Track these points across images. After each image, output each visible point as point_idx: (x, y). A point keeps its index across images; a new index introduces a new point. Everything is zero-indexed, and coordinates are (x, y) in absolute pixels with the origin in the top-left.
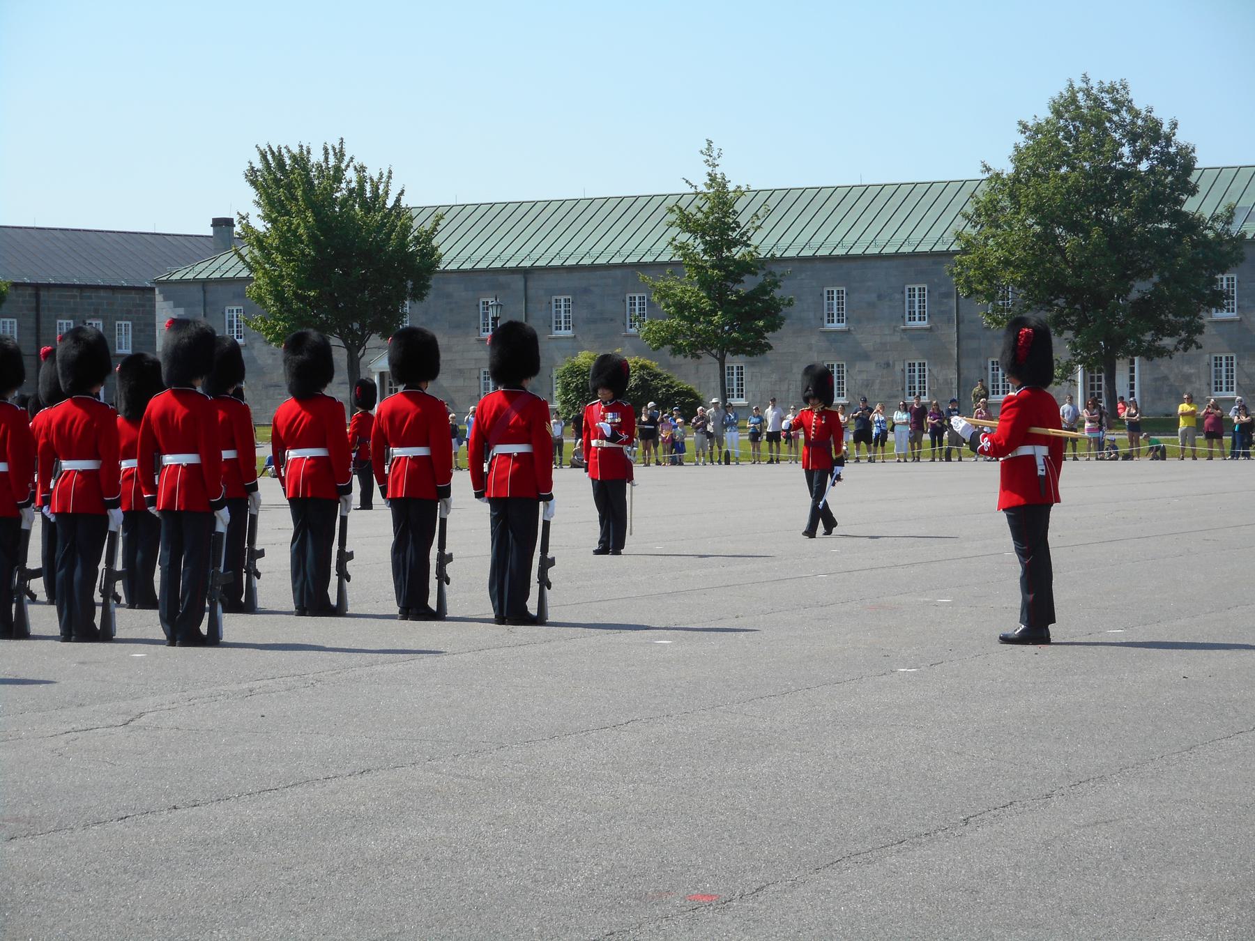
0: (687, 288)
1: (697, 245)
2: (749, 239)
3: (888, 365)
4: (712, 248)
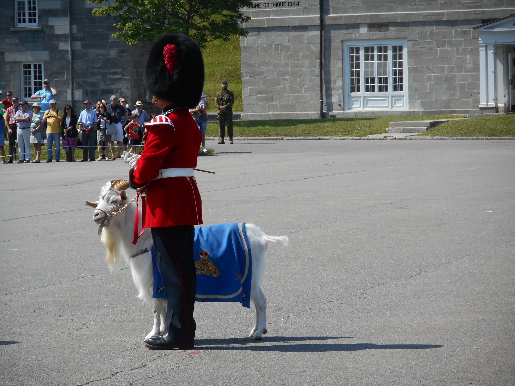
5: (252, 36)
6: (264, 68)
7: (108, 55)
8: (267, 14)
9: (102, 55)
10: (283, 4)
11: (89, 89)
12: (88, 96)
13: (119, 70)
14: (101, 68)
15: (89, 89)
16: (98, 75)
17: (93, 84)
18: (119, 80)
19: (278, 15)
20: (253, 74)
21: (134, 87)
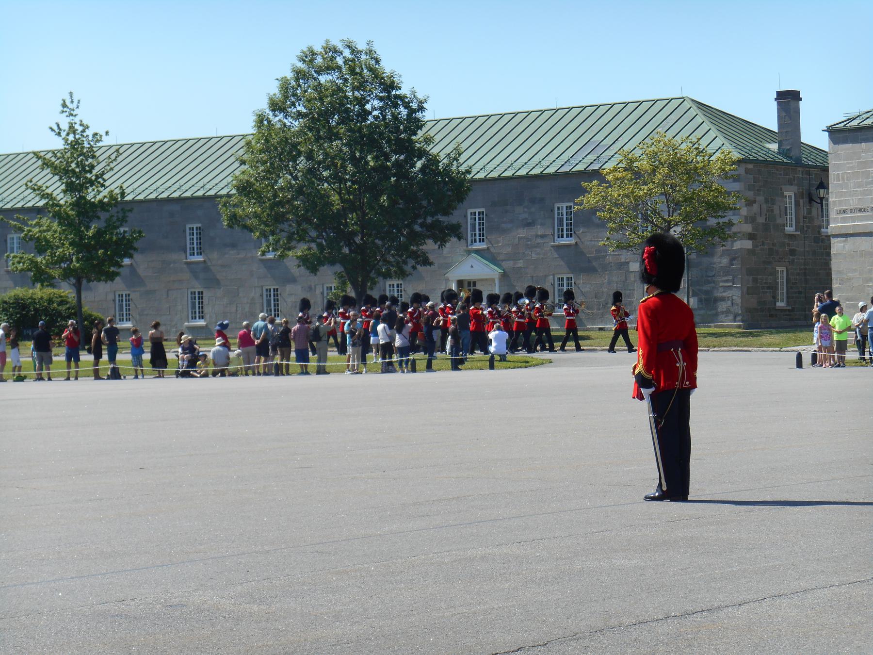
0: (49, 228)
1: (56, 187)
2: (105, 180)
3: (310, 288)
4: (70, 188)
5: (840, 242)
6: (850, 275)
7: (720, 263)
8: (853, 219)
10: (866, 210)
13: (730, 278)
15: (703, 296)
17: (707, 292)
19: (862, 221)
20: (842, 281)
21: (748, 294)
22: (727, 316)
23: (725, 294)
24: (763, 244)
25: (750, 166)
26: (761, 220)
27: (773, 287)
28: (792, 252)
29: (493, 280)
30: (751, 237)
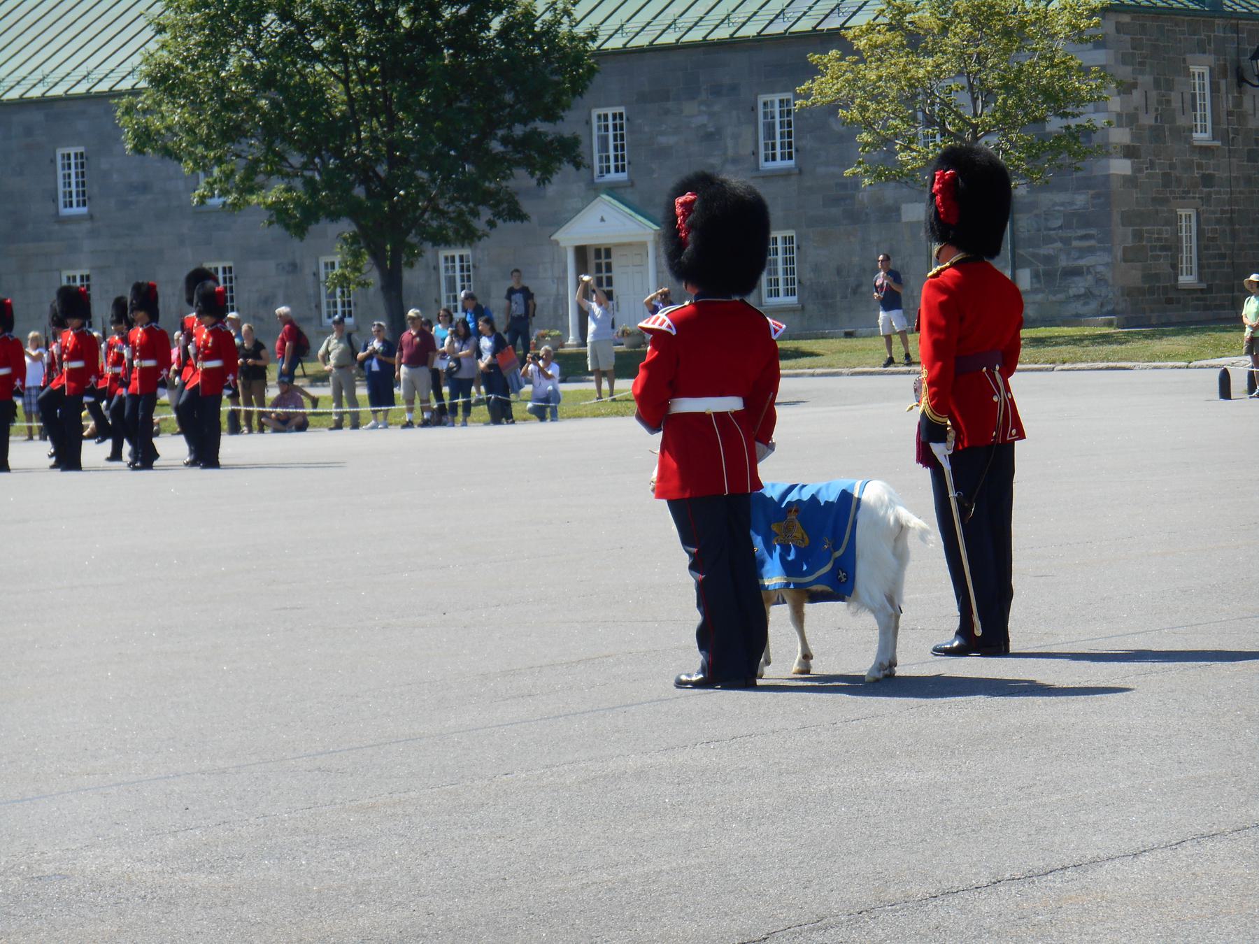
7: (1072, 203)
9: (1062, 204)
11: (1041, 268)
12: (1039, 281)
13: (1093, 231)
14: (1060, 228)
15: (1041, 268)
16: (1054, 241)
17: (1048, 259)
18: (1091, 250)
21: (1125, 260)
22: (1086, 304)
23: (1081, 263)
24: (1152, 165)
25: (1126, 19)
26: (1147, 120)
27: (1172, 248)
28: (1207, 180)
29: (643, 245)
30: (1129, 152)
